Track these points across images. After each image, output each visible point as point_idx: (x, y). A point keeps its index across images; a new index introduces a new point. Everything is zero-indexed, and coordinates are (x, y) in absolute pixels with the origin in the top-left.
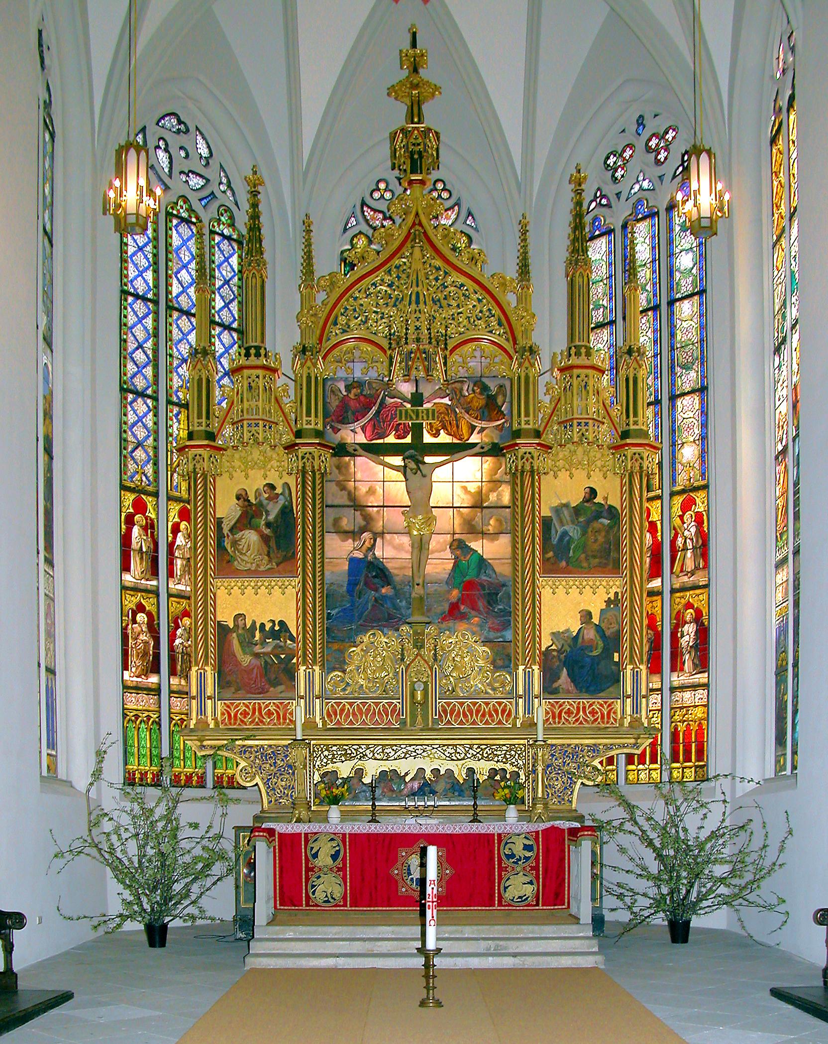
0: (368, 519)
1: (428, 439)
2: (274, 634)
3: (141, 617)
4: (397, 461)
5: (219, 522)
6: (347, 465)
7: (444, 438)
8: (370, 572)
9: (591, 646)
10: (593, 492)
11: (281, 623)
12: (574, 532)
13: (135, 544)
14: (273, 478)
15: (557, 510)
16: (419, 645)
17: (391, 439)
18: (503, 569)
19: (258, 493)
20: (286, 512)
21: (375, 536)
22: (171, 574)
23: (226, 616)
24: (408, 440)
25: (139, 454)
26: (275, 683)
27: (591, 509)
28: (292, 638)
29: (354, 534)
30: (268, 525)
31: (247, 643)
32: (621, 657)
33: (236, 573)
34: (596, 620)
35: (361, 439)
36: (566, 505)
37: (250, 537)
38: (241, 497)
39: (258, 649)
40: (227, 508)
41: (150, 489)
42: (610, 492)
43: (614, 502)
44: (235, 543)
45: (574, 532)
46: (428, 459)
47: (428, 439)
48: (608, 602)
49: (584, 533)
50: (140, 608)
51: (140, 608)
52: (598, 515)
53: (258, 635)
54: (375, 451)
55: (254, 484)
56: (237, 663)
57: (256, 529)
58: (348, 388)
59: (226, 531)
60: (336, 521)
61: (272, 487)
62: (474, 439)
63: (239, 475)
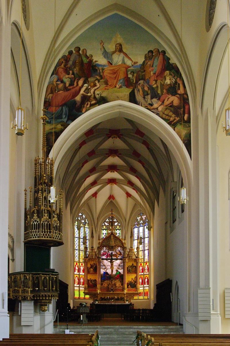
0: (106, 267)
1: (113, 258)
2: (94, 281)
3: (77, 278)
4: (109, 260)
5: (88, 267)
6: (103, 261)
7: (115, 258)
8: (106, 273)
9: (132, 282)
10: (133, 264)
11: (96, 280)
12: (131, 269)
13: (76, 269)
14: (95, 262)
15: (129, 266)
16: (112, 282)
17: (109, 258)
18: (122, 273)
19: (93, 264)
20: (96, 266)
21: (107, 269)
22: (80, 272)
23: (89, 279)
24: (111, 258)
25: (77, 257)
26: (94, 287)
27: (132, 266)
28: (97, 281)
29: (104, 269)
30: (94, 268)
31: (91, 282)
32: (136, 284)
33: (90, 274)
34: (133, 279)
35: (105, 258)
36: (130, 266)
37: (92, 269)
38: (91, 264)
39: (93, 283)
40: (89, 266)
41: (78, 262)
42: (135, 264)
43: (135, 265)
44: (90, 270)
45: (131, 269)
46: (113, 260)
47: (113, 258)
48: (135, 277)
49: (132, 269)
50: (77, 277)
51: (77, 277)
52: (133, 267)
53: (92, 281)
54: (106, 259)
55: (92, 263)
56: (90, 284)
57: (92, 268)
58: (104, 252)
59: (89, 268)
60: (102, 267)
61: (94, 263)
62: (119, 258)
63: (90, 262)
